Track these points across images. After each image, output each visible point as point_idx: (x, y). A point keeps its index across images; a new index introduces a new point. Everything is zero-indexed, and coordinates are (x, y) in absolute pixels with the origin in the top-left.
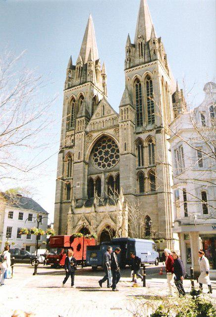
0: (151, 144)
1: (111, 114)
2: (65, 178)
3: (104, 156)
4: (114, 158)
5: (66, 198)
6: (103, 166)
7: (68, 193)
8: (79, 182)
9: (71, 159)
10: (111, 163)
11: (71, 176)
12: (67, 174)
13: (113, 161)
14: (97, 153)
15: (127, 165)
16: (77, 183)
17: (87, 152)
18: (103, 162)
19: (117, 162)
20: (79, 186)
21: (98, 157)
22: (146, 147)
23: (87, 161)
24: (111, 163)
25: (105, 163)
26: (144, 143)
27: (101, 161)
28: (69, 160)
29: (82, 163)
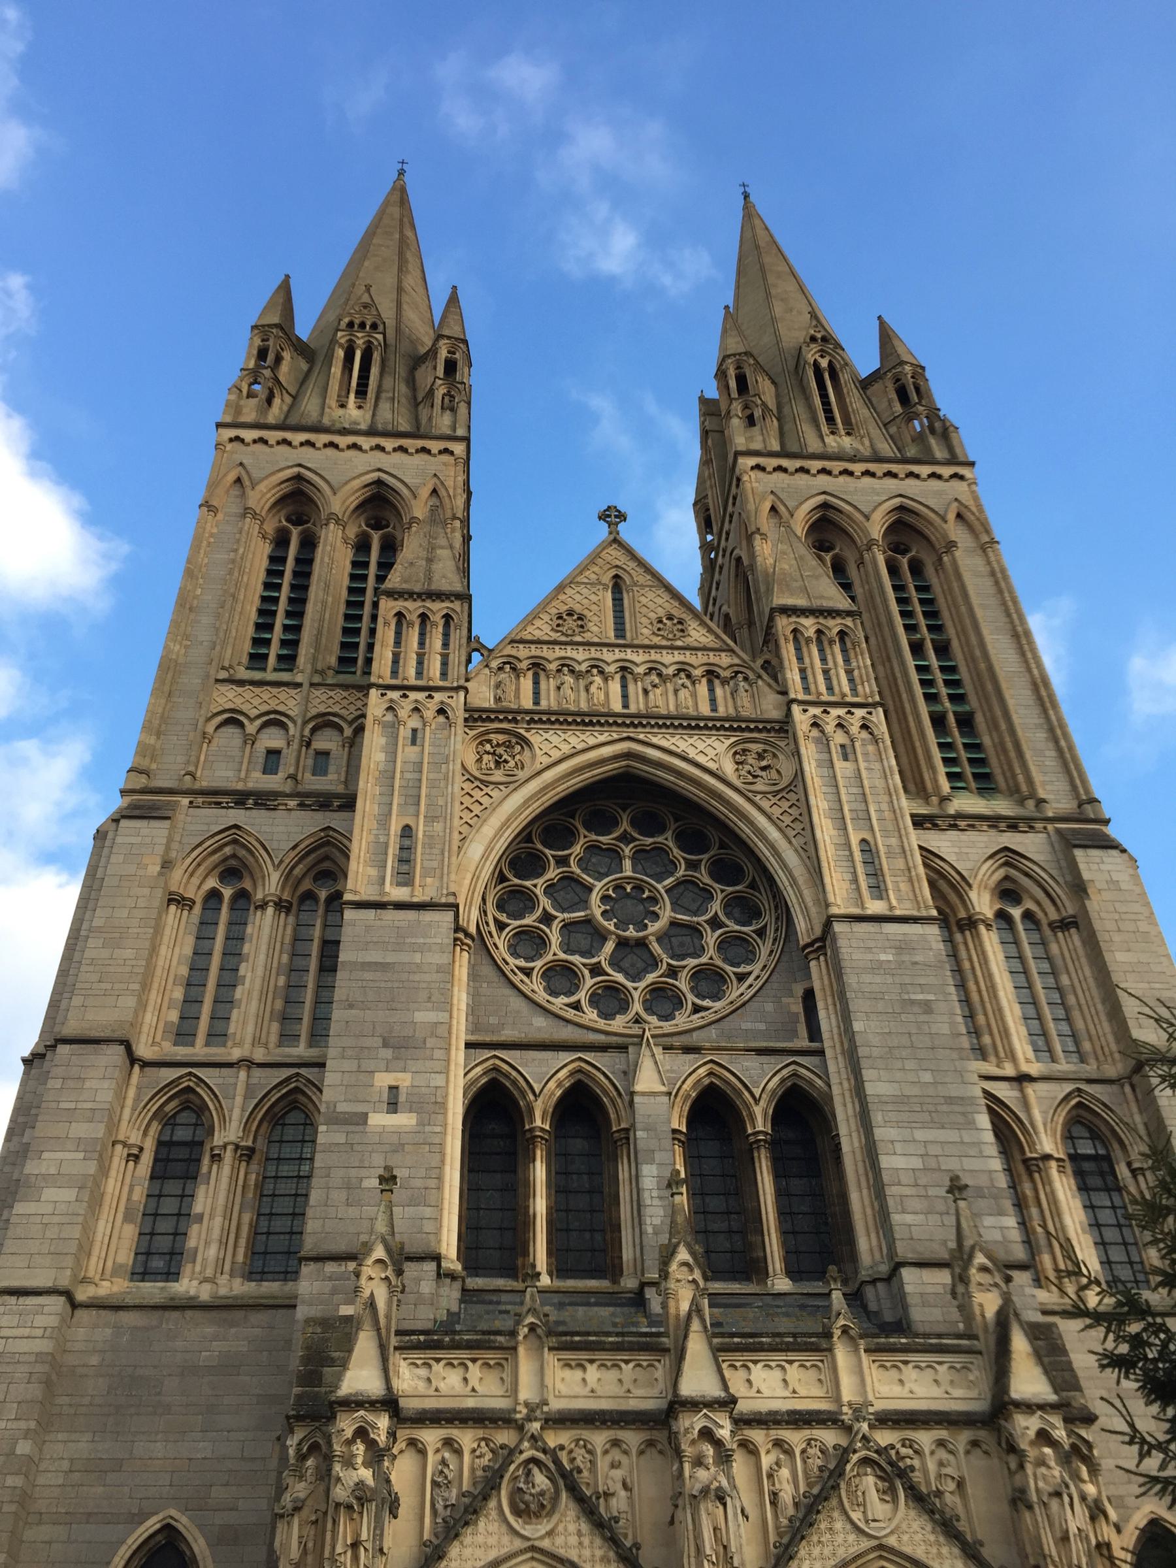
0: (1016, 913)
1: (689, 641)
2: (144, 1050)
3: (610, 925)
4: (710, 954)
5: (125, 1256)
6: (594, 1000)
7: (154, 1196)
8: (404, 1080)
9: (242, 896)
10: (683, 984)
11: (217, 1036)
12: (174, 1016)
13: (699, 974)
14: (538, 885)
15: (927, 1008)
16: (383, 1080)
17: (475, 850)
18: (596, 970)
19: (735, 992)
20: (404, 1120)
21: (547, 919)
22: (988, 927)
23: (471, 918)
24: (683, 984)
25: (620, 977)
26: (973, 895)
27: (576, 959)
28: (214, 895)
29: (449, 916)
